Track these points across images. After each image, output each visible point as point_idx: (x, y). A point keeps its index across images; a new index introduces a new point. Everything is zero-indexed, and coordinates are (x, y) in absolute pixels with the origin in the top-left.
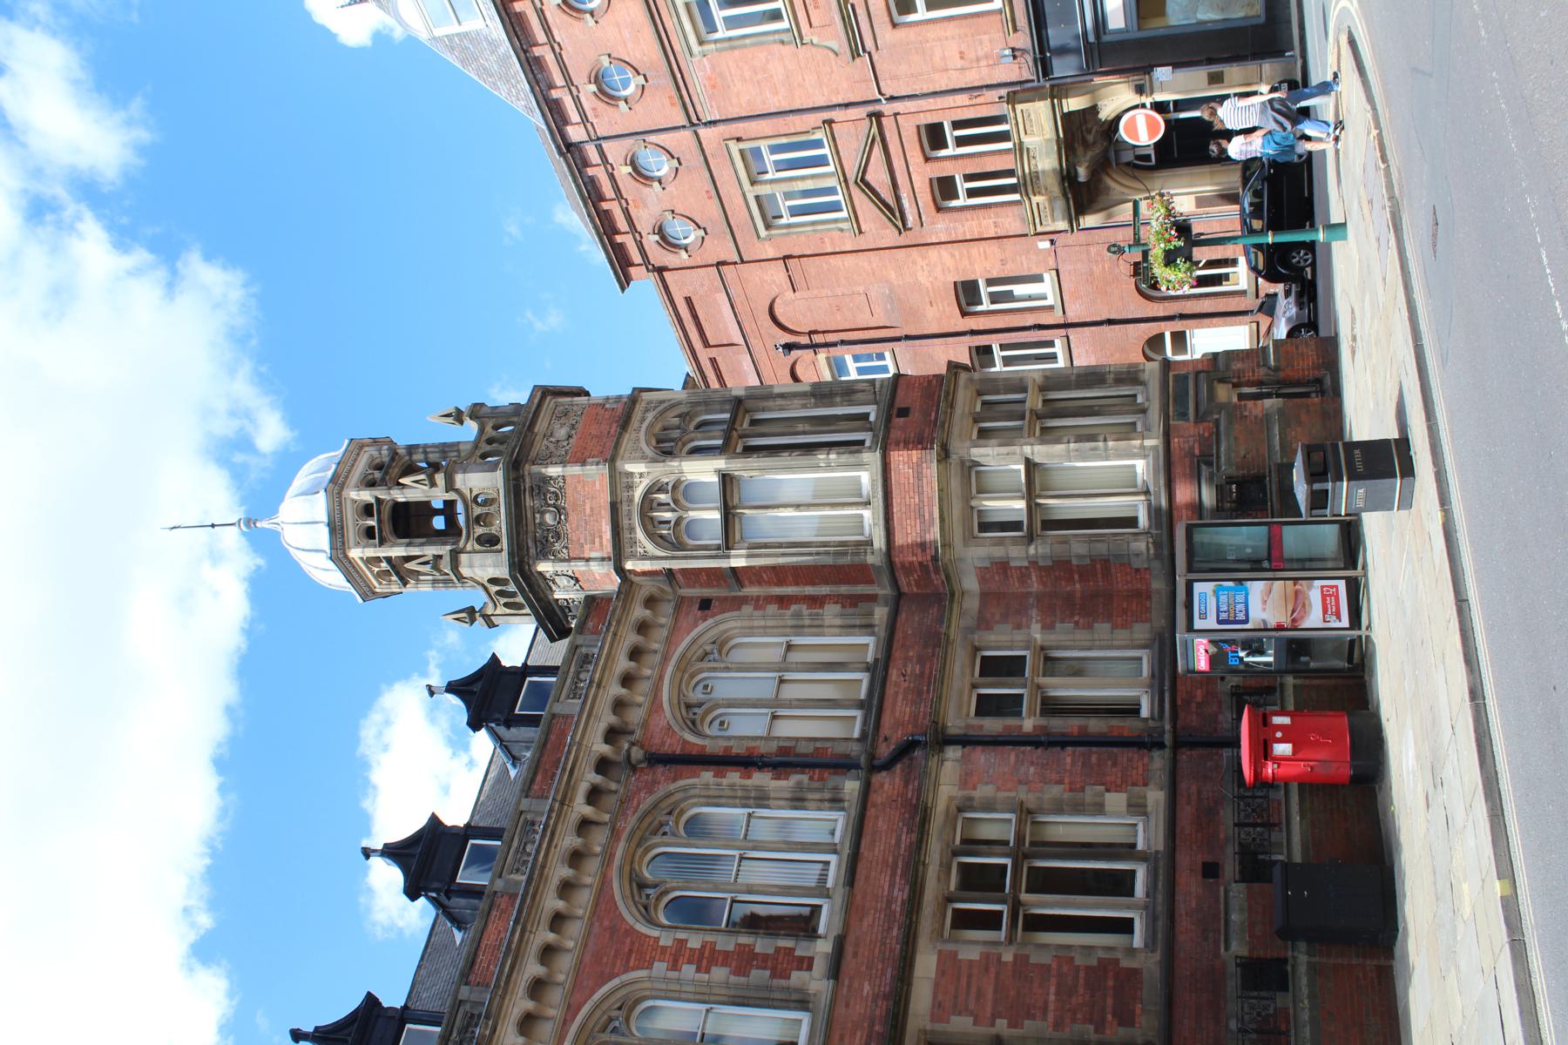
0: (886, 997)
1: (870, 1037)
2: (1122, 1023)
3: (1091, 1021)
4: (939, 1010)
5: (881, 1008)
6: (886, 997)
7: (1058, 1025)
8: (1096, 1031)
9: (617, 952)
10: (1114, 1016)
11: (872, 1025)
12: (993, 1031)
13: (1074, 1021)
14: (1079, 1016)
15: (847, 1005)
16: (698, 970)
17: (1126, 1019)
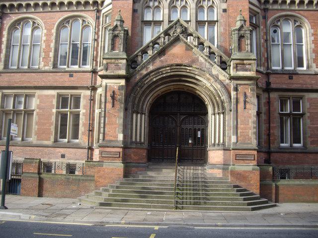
0: (312, 87)
1: (303, 84)
2: (311, 142)
3: (311, 135)
4: (310, 100)
5: (310, 87)
6: (312, 87)
7: (309, 127)
8: (309, 136)
9: (315, 20)
10: (313, 140)
11: (305, 84)
12: (306, 113)
13: (311, 131)
14: (312, 132)
15: (309, 78)
16: (313, 41)
17: (313, 143)
